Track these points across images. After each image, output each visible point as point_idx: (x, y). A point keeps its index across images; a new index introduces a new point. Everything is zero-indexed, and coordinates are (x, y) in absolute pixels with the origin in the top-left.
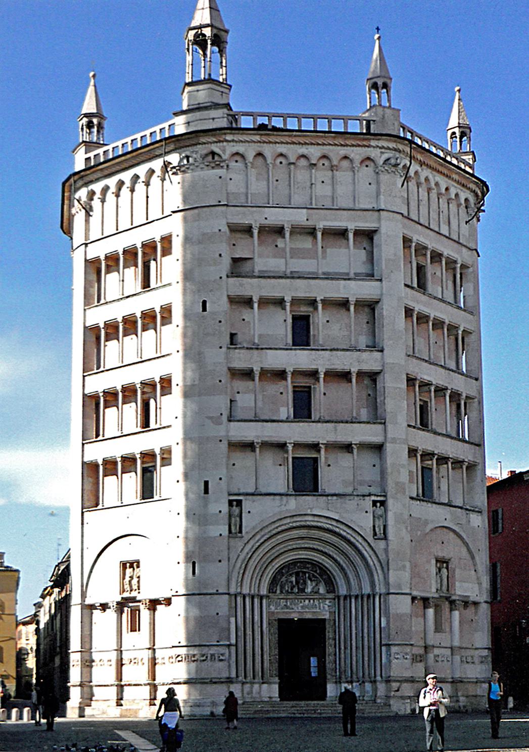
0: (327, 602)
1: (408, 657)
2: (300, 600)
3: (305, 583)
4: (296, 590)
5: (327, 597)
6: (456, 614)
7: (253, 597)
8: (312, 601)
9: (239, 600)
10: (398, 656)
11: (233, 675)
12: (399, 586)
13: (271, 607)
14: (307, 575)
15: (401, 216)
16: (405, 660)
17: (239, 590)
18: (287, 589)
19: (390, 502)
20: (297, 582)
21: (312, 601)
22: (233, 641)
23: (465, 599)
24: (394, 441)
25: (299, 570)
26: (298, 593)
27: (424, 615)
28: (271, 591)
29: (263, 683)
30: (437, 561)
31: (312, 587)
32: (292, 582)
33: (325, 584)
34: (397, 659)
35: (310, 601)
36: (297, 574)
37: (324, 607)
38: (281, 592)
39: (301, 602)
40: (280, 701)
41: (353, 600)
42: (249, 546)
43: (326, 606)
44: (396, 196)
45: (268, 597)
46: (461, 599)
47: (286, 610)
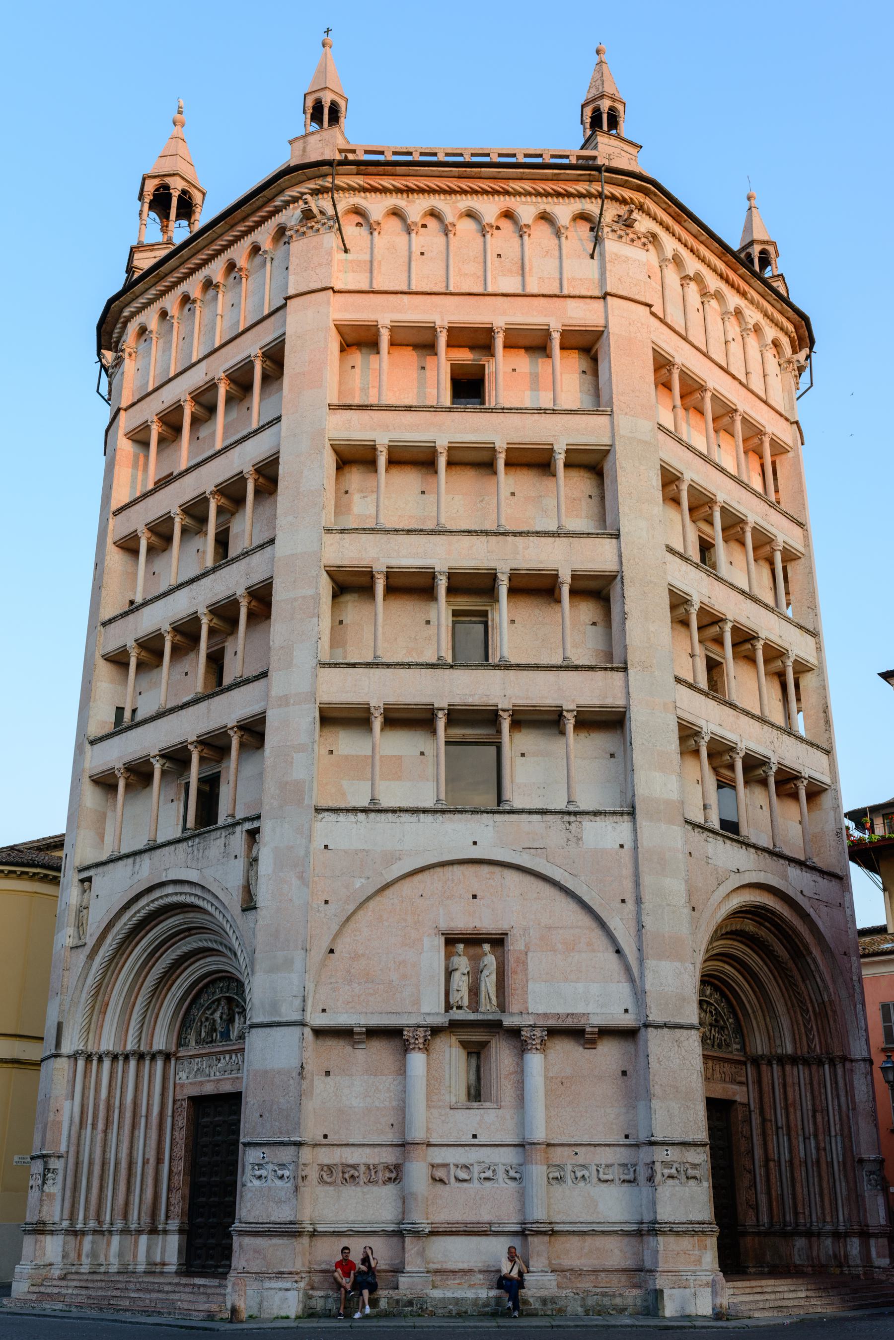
1: (287, 1173)
6: (535, 1061)
7: (127, 1058)
9: (81, 1063)
10: (263, 1172)
11: (57, 1219)
12: (275, 1006)
15: (337, 288)
16: (279, 1183)
17: (81, 1047)
19: (267, 827)
22: (63, 1149)
23: (569, 1022)
24: (285, 701)
27: (402, 1071)
29: (139, 1232)
30: (451, 941)
34: (260, 1177)
35: (231, 1058)
40: (178, 1273)
42: (98, 960)
44: (320, 265)
45: (167, 1057)
46: (541, 1022)
47: (200, 1079)
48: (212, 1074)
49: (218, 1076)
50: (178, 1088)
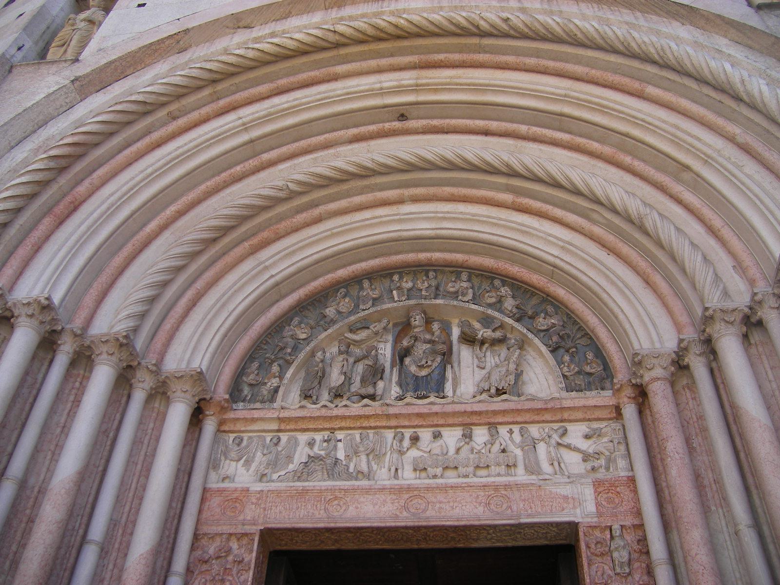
0: (576, 433)
2: (408, 433)
3: (447, 356)
4: (390, 387)
5: (567, 404)
8: (481, 435)
13: (230, 467)
14: (456, 332)
18: (335, 378)
20: (401, 355)
21: (481, 435)
25: (412, 302)
26: (400, 398)
28: (246, 390)
31: (480, 374)
32: (370, 353)
33: (554, 351)
36: (404, 328)
37: (556, 462)
38: (306, 396)
39: (415, 439)
41: (731, 349)
43: (573, 461)
48: (383, 476)
49: (408, 476)
50: (215, 502)
